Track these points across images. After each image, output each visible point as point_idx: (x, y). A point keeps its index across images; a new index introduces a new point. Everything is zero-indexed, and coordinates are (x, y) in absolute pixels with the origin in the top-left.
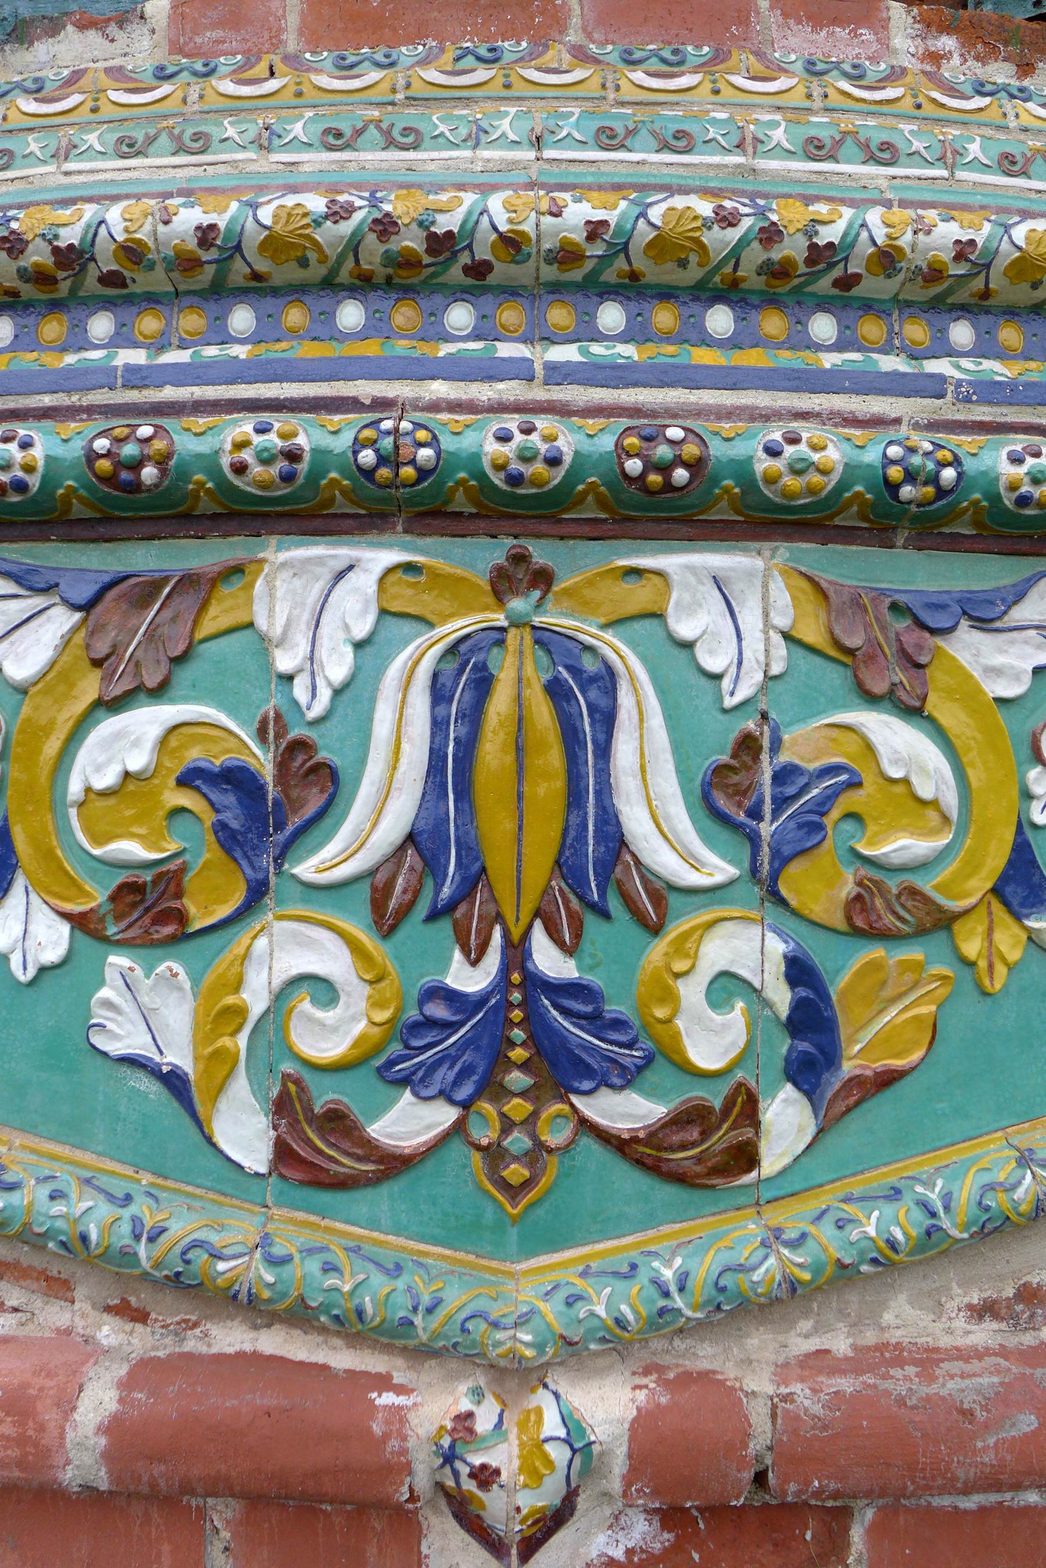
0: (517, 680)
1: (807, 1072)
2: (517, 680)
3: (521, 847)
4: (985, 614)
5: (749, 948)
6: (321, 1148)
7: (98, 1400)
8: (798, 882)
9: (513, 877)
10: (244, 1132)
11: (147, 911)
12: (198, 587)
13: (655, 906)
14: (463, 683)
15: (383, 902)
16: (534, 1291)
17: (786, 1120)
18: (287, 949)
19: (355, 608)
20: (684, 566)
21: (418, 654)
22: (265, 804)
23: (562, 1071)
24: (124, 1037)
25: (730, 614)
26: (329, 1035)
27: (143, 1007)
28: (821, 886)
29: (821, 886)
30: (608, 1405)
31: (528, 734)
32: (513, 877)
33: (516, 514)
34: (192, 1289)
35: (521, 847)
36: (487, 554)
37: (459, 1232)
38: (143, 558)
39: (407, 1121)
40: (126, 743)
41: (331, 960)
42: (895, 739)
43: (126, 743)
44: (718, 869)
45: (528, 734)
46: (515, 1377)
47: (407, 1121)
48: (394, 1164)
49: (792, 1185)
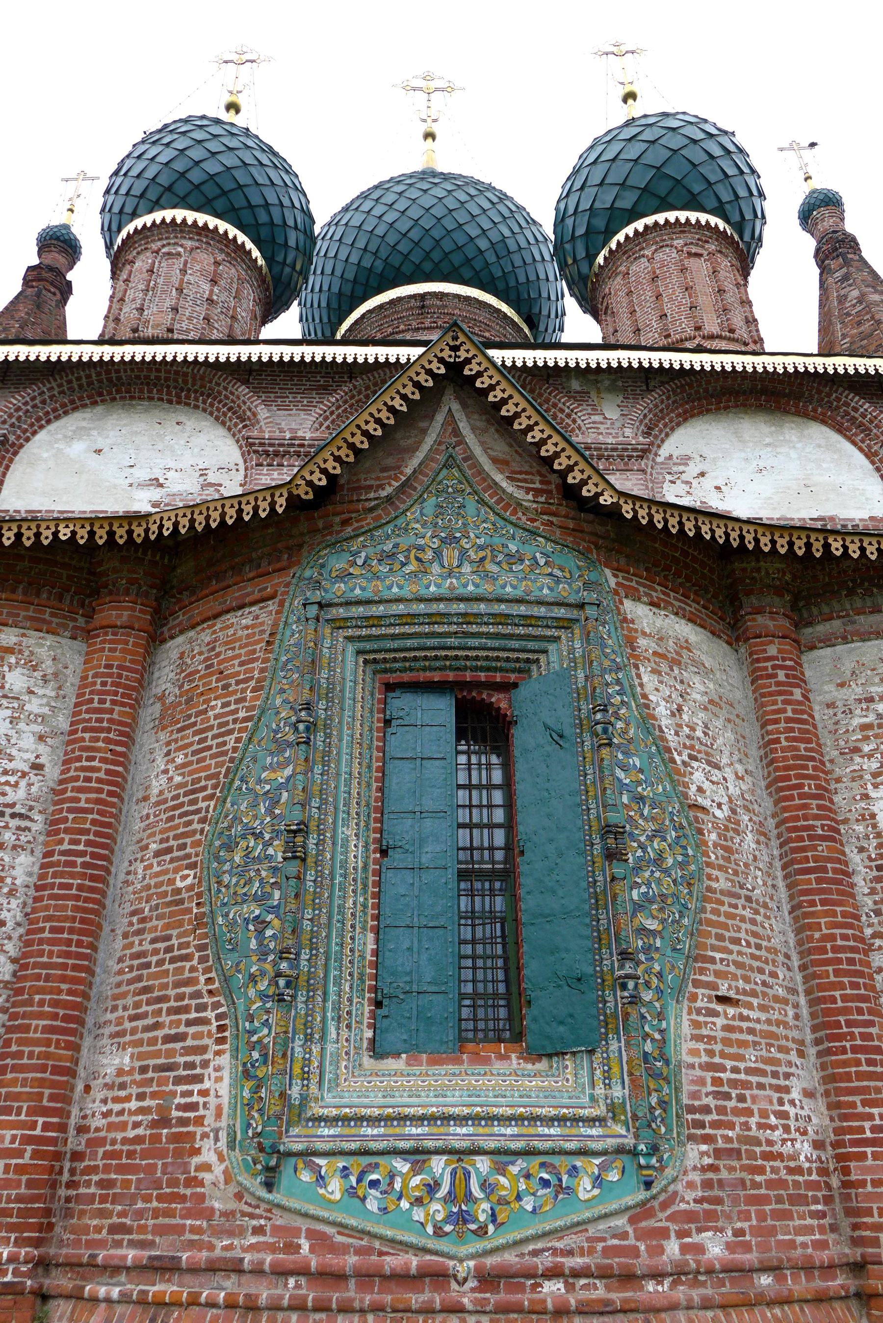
0: (460, 1172)
1: (494, 1221)
2: (460, 1172)
3: (461, 1193)
4: (513, 1163)
5: (486, 1206)
6: (439, 1232)
7: (415, 1263)
8: (492, 1198)
9: (460, 1194)
10: (430, 1230)
11: (419, 1201)
12: (424, 1161)
13: (476, 1201)
14: (454, 1173)
15: (445, 1200)
16: (464, 1250)
17: (491, 1228)
18: (435, 1206)
19: (442, 1164)
20: (477, 1158)
21: (449, 1170)
22: (432, 1188)
23: (465, 1222)
24: (416, 1218)
25: (483, 1164)
26: (440, 1217)
27: (418, 1214)
28: (494, 1198)
29: (494, 1198)
30: (472, 1263)
31: (461, 1178)
32: (460, 1194)
33: (459, 1154)
34: (426, 1250)
35: (461, 1193)
36: (456, 1157)
37: (454, 1243)
38: (418, 1157)
39: (448, 1228)
40: (416, 1181)
41: (439, 1207)
42: (502, 1180)
43: (416, 1181)
44: (482, 1196)
45: (461, 1178)
46: (461, 1261)
47: (448, 1228)
48: (447, 1234)
49: (492, 1237)
